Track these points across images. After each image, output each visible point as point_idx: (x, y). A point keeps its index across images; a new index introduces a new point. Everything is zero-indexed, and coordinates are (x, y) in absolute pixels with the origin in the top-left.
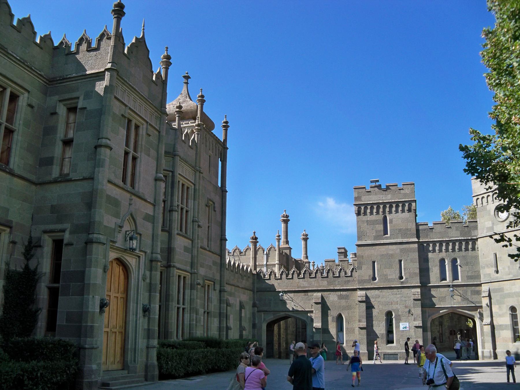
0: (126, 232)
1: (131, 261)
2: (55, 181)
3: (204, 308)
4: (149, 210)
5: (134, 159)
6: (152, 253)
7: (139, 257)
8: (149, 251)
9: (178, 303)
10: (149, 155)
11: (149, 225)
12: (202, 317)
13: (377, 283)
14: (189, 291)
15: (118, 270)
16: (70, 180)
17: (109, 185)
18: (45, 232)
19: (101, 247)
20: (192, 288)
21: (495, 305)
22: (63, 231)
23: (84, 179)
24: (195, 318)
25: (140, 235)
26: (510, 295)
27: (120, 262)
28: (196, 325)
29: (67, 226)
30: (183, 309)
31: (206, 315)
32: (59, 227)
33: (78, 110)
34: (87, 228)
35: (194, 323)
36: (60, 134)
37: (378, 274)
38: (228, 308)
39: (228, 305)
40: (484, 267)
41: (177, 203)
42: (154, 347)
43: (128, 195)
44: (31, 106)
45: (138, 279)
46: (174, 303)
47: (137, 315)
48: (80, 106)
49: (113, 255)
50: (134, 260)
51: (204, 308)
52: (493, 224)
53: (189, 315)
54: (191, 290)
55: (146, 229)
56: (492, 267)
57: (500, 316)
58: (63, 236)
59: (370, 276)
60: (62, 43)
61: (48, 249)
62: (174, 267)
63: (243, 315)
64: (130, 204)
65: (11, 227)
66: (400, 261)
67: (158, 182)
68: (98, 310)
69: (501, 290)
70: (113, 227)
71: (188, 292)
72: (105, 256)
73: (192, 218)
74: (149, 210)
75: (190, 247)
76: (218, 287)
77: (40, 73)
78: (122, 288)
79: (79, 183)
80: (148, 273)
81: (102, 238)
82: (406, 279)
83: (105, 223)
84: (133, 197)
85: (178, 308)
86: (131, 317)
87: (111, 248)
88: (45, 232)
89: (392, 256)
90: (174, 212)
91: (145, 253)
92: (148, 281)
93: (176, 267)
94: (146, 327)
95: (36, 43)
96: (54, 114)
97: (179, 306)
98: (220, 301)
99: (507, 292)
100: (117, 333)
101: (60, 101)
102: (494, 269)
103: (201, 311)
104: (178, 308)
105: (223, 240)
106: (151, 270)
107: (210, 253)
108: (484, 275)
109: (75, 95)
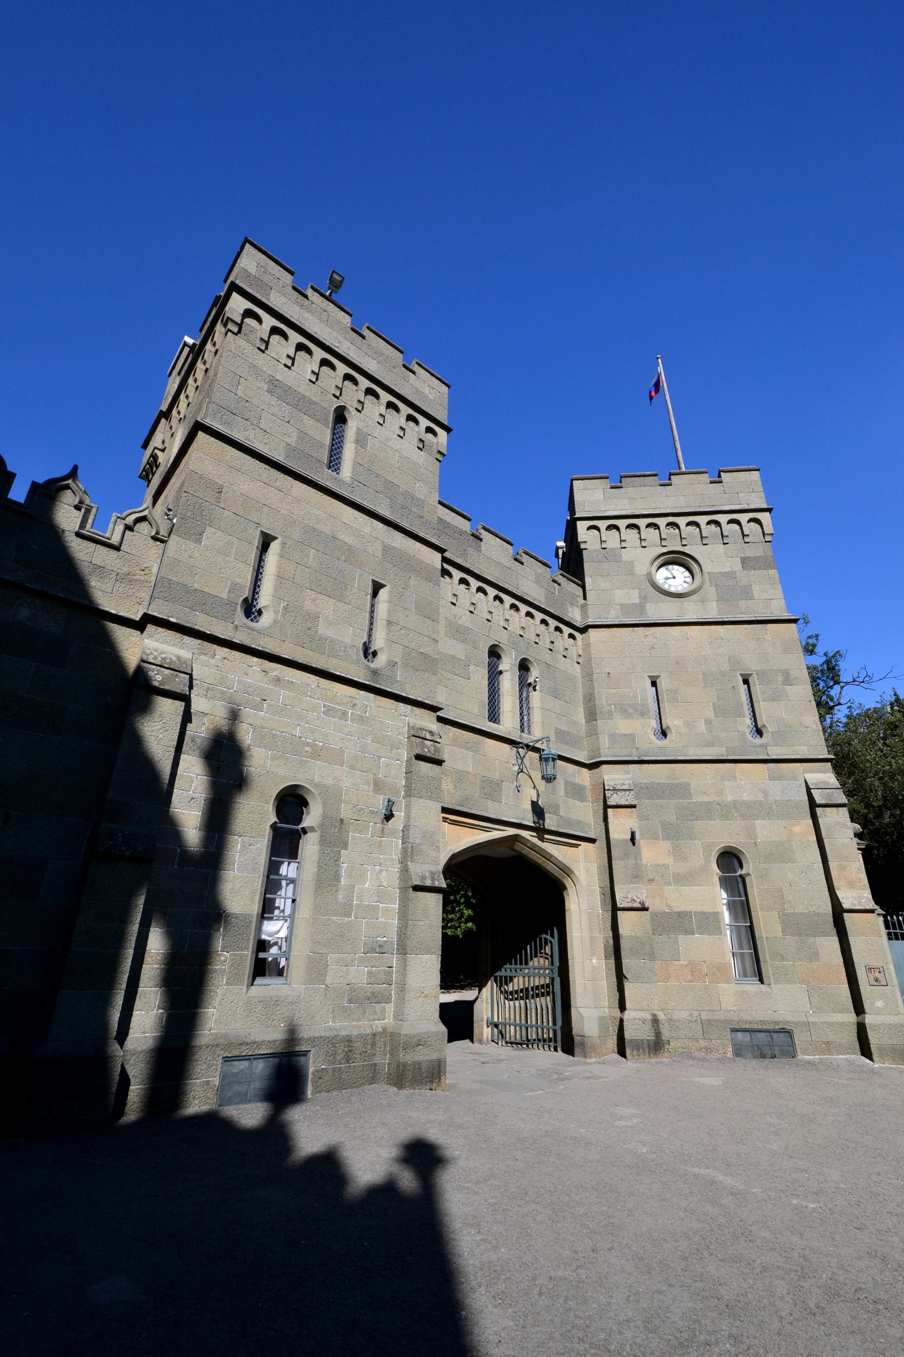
13: (264, 632)
21: (657, 838)
26: (725, 811)
37: (276, 597)
40: (610, 713)
52: (644, 598)
56: (643, 714)
57: (680, 879)
59: (234, 587)
66: (377, 588)
69: (679, 790)
82: (392, 664)
89: (350, 553)
99: (707, 799)
102: (654, 723)
108: (612, 736)
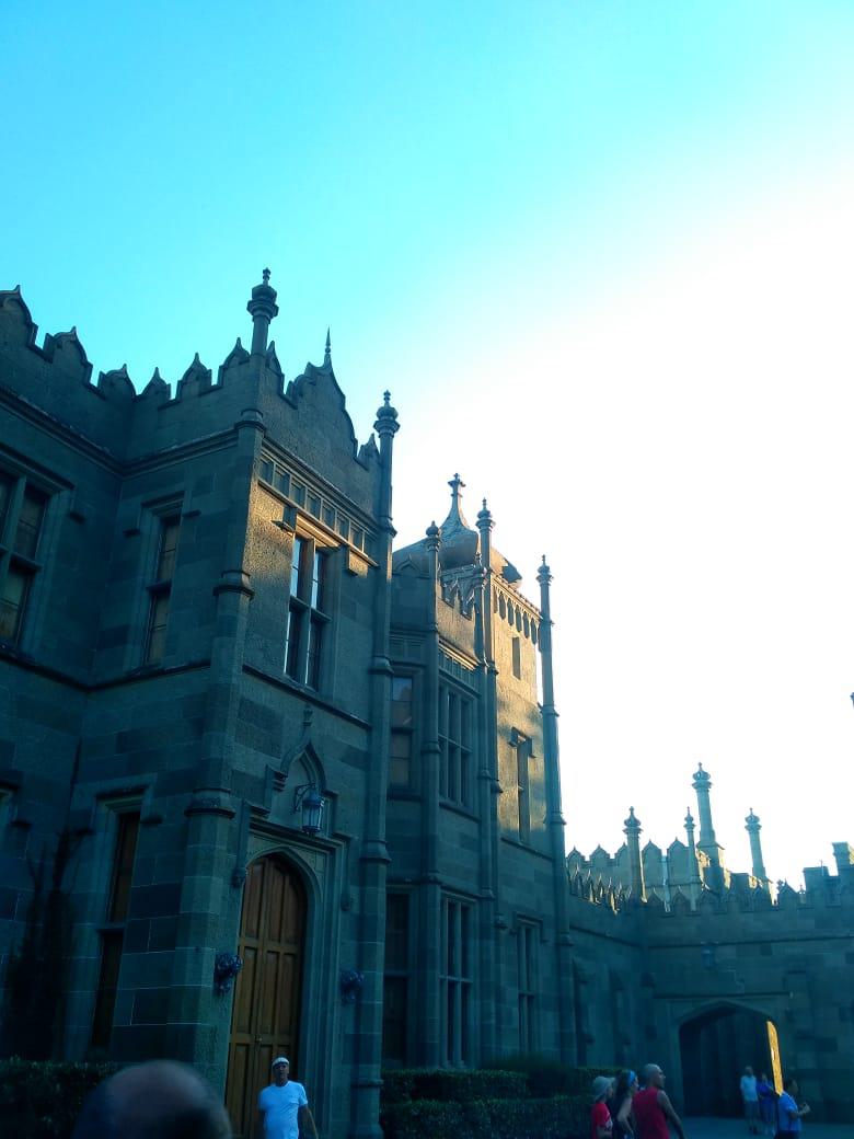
0: (297, 789)
1: (314, 862)
2: (131, 679)
3: (520, 985)
4: (356, 739)
5: (319, 623)
6: (366, 841)
7: (332, 851)
8: (356, 837)
9: (451, 972)
10: (353, 617)
11: (356, 774)
12: (515, 1010)
14: (478, 941)
15: (277, 883)
16: (163, 673)
17: (251, 680)
18: (101, 797)
19: (222, 824)
20: (484, 935)
22: (140, 790)
23: (192, 666)
24: (493, 1010)
25: (333, 796)
27: (282, 863)
28: (498, 1029)
29: (149, 777)
30: (466, 987)
31: (525, 1004)
32: (135, 781)
33: (182, 518)
34: (197, 777)
35: (493, 1021)
36: (146, 576)
38: (583, 988)
39: (579, 981)
41: (438, 734)
42: (372, 1085)
43: (301, 704)
44: (76, 517)
45: (330, 905)
46: (438, 972)
47: (325, 998)
48: (185, 510)
49: (257, 847)
50: (320, 859)
51: (520, 985)
53: (478, 1002)
54: (481, 938)
55: (345, 780)
58: (140, 803)
60: (150, 386)
61: (103, 841)
62: (436, 882)
63: (620, 1003)
64: (306, 725)
65: (15, 788)
67: (378, 678)
68: (208, 983)
70: (261, 774)
71: (474, 944)
72: (238, 847)
73: (477, 770)
74: (356, 739)
75: (475, 835)
76: (550, 934)
77: (100, 448)
78: (289, 932)
79: (179, 676)
80: (354, 892)
81: (226, 800)
83: (239, 766)
84: (313, 708)
85: (452, 985)
86: (312, 1006)
87: (252, 826)
88: (101, 797)
90: (432, 756)
91: (347, 839)
92: (355, 909)
93: (440, 883)
94: (350, 1030)
95: (91, 387)
96: (133, 533)
97: (454, 979)
98: (559, 967)
100: (275, 1048)
101: (145, 505)
103: (512, 994)
104: (452, 985)
105: (555, 823)
106: (362, 882)
107: (527, 854)
109: (177, 488)
